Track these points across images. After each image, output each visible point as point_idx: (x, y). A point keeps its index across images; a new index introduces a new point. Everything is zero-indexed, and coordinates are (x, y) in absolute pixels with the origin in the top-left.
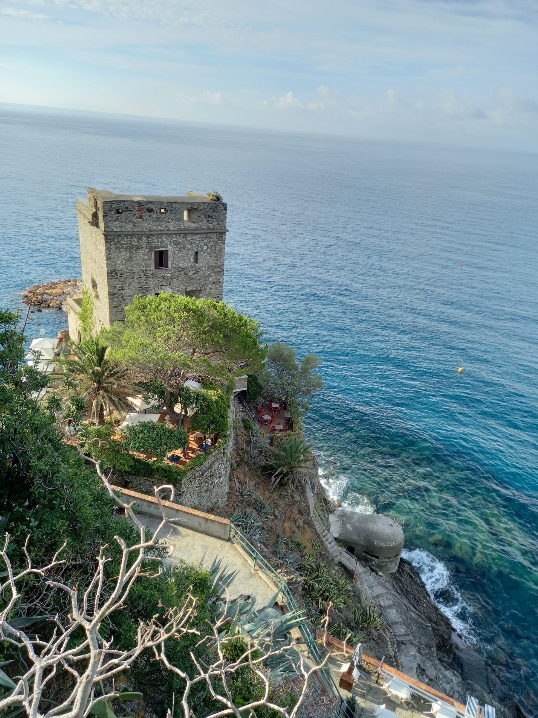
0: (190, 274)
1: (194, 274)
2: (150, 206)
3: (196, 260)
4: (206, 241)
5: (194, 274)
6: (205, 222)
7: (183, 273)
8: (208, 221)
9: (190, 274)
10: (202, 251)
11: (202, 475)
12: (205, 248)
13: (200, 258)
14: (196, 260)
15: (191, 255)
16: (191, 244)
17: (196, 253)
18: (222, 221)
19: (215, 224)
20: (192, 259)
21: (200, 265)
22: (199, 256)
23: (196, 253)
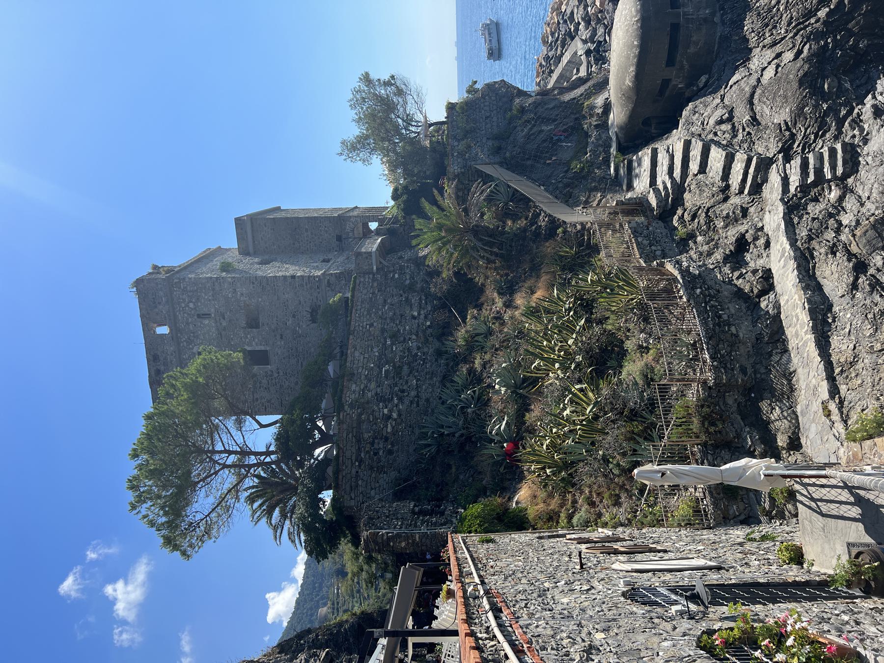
0: (224, 324)
1: (224, 318)
2: (153, 373)
3: (207, 315)
4: (183, 305)
5: (224, 318)
6: (161, 307)
7: (223, 333)
8: (160, 303)
9: (224, 324)
10: (195, 309)
11: (361, 461)
12: (191, 305)
13: (205, 311)
14: (207, 315)
15: (201, 323)
16: (188, 324)
17: (199, 316)
18: (157, 284)
19: (161, 293)
20: (206, 322)
21: (213, 310)
22: (202, 312)
23: (199, 316)
